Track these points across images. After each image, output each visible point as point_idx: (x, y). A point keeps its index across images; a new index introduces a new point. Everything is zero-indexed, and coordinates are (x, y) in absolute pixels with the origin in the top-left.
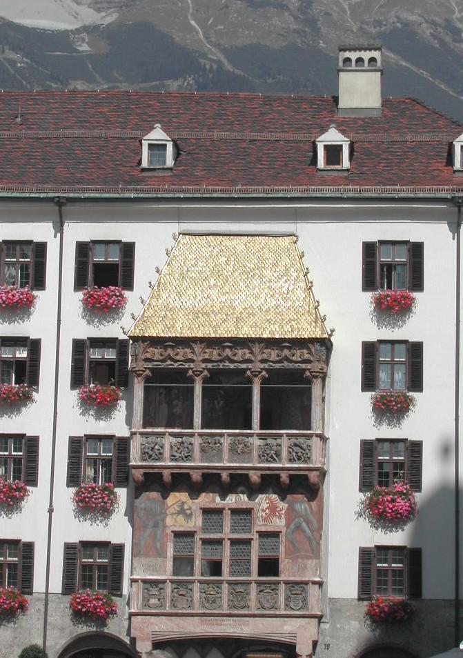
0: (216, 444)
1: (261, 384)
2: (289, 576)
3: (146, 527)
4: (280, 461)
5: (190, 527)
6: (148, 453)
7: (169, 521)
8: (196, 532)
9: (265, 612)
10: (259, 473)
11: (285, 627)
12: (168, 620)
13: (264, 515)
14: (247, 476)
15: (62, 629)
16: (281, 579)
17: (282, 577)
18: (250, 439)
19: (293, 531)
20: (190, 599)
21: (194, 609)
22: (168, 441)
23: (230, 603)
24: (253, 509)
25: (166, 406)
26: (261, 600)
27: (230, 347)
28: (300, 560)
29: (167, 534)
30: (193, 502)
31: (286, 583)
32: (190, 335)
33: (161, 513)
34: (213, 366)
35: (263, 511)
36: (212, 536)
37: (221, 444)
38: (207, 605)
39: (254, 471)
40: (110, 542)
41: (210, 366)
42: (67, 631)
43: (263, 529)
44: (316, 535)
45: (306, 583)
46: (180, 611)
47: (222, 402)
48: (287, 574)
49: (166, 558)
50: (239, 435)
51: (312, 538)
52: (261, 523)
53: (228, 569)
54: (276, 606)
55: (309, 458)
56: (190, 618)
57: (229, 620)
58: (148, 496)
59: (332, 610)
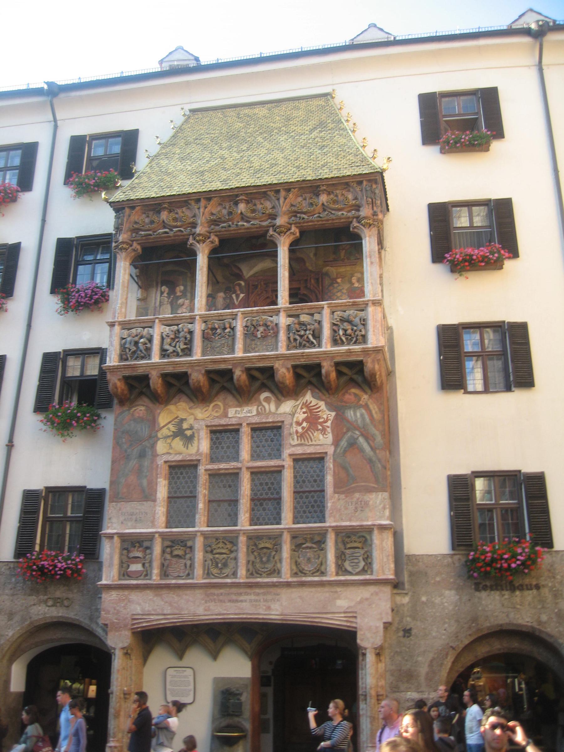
0: (225, 329)
1: (291, 245)
2: (342, 519)
3: (127, 458)
4: (320, 346)
5: (191, 455)
6: (130, 350)
7: (161, 447)
8: (199, 460)
9: (304, 579)
10: (289, 364)
11: (339, 603)
12: (156, 595)
13: (300, 429)
14: (271, 368)
15: (11, 615)
16: (327, 524)
17: (330, 522)
18: (274, 318)
19: (345, 451)
20: (188, 563)
21: (193, 578)
22: (157, 331)
23: (250, 567)
24: (283, 422)
25: (169, 307)
26: (299, 560)
27: (247, 202)
28: (357, 495)
29: (158, 466)
30: (196, 419)
31: (338, 531)
32: (190, 191)
33: (150, 437)
34: (222, 227)
35: (299, 424)
36: (222, 466)
37: (233, 329)
39: (281, 362)
40: (85, 487)
41: (217, 228)
42: (17, 618)
43: (299, 450)
44: (381, 454)
45: (369, 530)
46: (173, 581)
47: (242, 295)
48: (337, 516)
49: (154, 501)
50: (257, 312)
51: (374, 459)
53: (247, 515)
54: (323, 568)
55: (364, 337)
56: (188, 592)
57: (247, 594)
58: (133, 415)
59: (411, 574)
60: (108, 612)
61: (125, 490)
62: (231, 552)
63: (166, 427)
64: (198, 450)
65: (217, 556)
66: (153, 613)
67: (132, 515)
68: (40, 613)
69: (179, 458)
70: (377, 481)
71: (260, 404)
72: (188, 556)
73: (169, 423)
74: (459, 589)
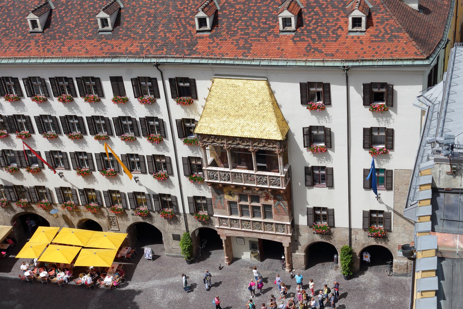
15: (193, 226)
41: (232, 146)
42: (194, 226)
43: (264, 203)
62: (249, 223)
70: (286, 213)
71: (252, 190)
74: (309, 233)
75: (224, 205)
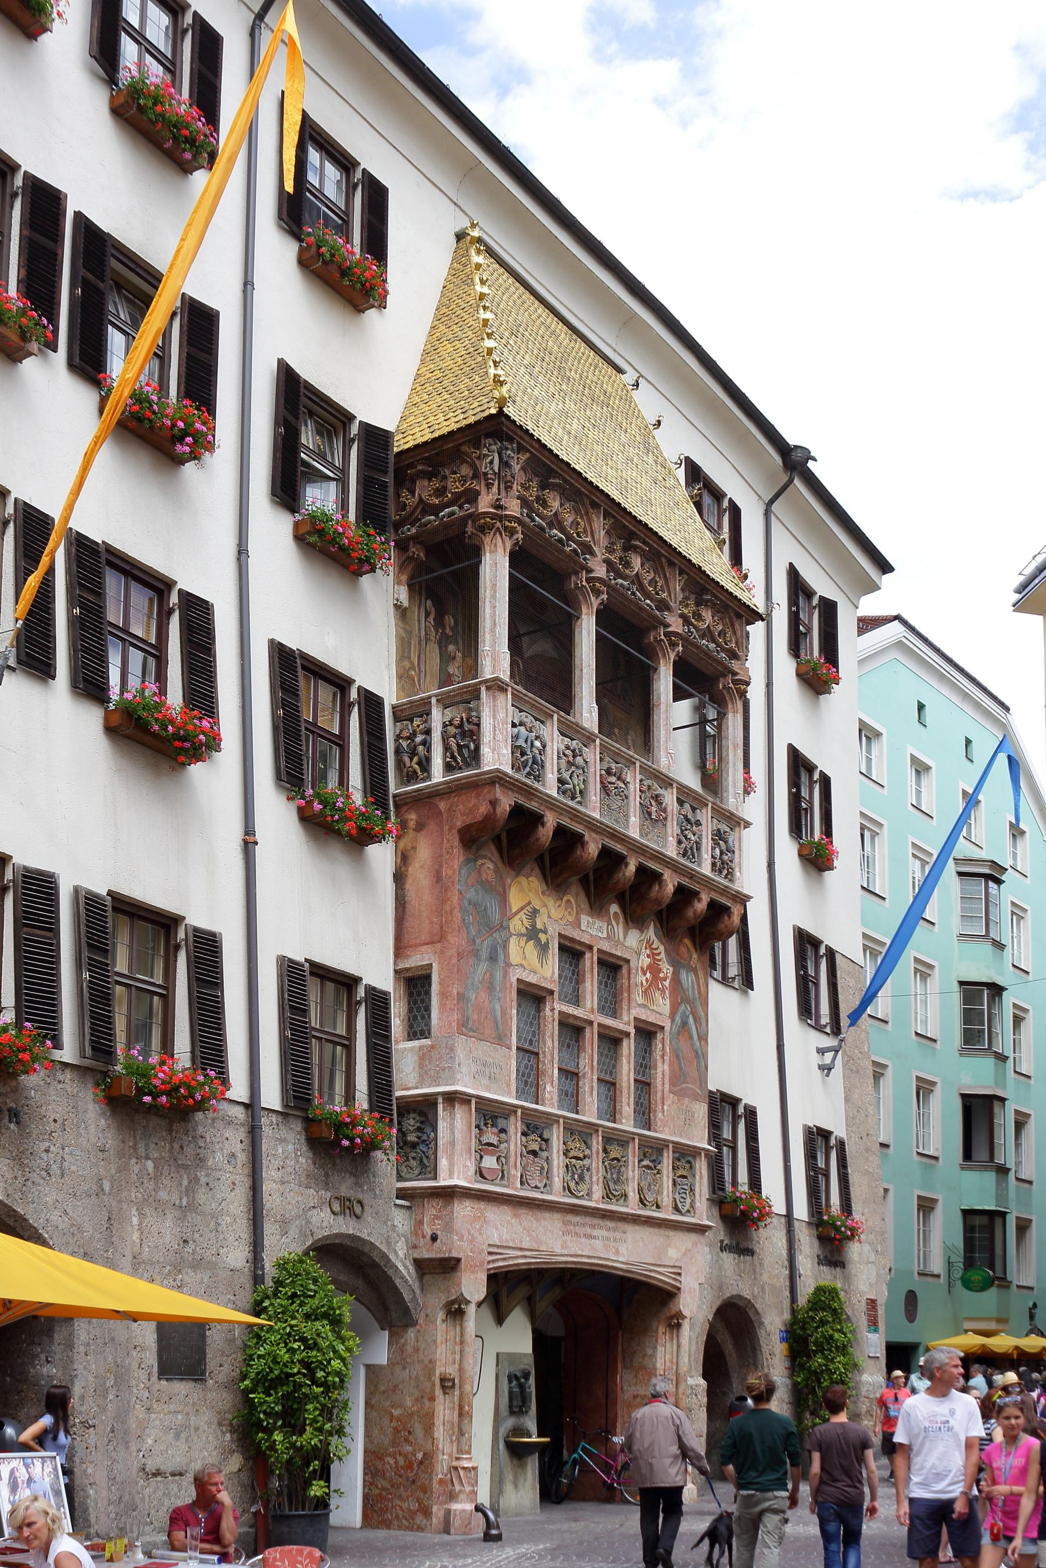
12: (515, 1216)
24: (628, 961)
30: (549, 917)
38: (572, 1185)
42: (294, 1232)
52: (640, 1000)
57: (601, 1228)
60: (462, 1237)
61: (475, 1017)
63: (518, 916)
64: (553, 973)
65: (574, 1161)
66: (511, 1245)
67: (484, 1065)
68: (324, 1225)
69: (532, 979)
72: (544, 1154)
73: (522, 909)
75: (504, 1012)
